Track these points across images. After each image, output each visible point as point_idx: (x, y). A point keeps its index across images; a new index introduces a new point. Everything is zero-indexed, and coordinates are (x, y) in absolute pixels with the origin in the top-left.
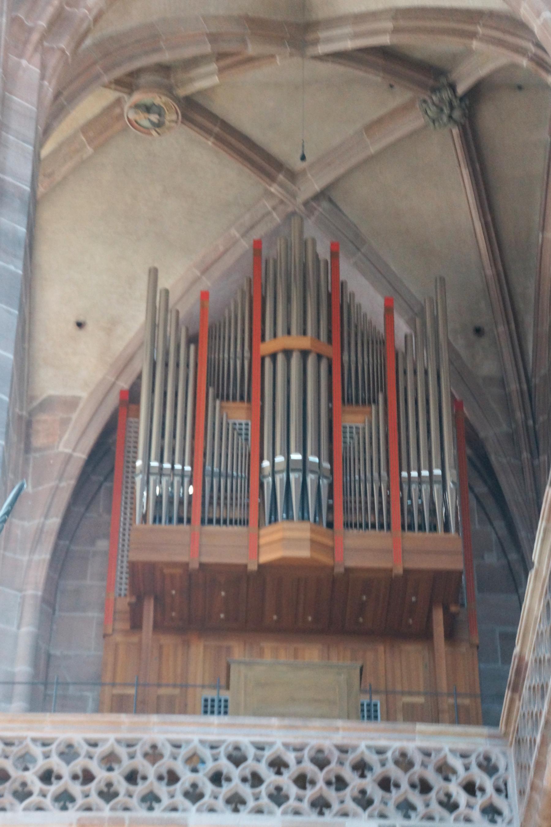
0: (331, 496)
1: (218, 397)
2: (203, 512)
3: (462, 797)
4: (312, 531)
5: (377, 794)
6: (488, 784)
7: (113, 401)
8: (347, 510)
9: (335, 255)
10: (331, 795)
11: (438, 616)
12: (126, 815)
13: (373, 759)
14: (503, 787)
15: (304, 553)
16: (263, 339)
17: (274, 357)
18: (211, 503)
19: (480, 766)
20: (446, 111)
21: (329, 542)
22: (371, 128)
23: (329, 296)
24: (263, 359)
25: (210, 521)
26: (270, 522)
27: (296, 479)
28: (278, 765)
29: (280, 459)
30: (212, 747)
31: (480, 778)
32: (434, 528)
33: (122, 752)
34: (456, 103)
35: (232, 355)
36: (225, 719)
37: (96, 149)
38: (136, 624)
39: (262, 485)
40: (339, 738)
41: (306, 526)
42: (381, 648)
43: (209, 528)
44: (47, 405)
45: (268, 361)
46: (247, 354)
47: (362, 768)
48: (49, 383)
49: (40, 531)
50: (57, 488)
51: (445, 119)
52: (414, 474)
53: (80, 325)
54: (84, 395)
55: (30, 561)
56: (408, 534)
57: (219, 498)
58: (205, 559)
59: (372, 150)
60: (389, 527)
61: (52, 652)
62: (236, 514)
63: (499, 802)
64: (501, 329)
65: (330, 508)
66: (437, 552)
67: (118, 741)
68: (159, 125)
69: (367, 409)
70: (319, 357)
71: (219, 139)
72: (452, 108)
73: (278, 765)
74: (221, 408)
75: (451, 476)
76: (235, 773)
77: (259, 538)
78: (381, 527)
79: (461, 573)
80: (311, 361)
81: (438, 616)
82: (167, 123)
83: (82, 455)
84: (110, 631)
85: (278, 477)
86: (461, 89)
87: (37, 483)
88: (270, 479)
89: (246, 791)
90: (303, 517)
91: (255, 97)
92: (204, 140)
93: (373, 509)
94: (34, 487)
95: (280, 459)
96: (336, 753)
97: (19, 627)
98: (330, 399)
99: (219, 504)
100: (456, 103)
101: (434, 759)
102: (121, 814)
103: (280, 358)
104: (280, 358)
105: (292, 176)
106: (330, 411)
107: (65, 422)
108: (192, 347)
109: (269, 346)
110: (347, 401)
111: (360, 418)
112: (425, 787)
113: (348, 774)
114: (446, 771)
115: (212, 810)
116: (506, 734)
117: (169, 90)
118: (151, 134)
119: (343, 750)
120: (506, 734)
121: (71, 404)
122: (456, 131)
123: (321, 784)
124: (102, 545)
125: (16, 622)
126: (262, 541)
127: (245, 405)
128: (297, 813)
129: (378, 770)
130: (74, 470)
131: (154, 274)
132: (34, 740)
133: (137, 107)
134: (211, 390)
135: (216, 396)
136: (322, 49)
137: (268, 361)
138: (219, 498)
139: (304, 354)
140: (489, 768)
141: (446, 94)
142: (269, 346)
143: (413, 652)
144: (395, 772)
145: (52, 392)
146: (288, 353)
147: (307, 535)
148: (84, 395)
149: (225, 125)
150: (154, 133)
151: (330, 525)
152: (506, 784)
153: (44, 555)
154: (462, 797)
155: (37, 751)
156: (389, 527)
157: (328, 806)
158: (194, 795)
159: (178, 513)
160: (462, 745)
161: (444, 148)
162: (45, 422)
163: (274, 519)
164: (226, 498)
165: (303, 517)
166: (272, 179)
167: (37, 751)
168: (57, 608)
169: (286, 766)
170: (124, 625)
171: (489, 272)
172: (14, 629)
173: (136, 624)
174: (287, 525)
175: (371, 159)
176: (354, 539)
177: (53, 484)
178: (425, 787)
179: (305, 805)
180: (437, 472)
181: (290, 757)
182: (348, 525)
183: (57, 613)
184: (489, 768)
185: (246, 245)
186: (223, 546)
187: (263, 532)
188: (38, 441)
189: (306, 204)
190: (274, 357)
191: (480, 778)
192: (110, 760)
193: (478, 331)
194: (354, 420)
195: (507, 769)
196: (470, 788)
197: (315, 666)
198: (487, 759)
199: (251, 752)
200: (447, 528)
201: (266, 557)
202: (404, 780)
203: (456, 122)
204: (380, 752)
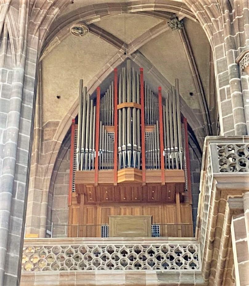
0: (141, 157)
1: (103, 124)
2: (99, 164)
3: (183, 261)
4: (135, 171)
5: (156, 261)
6: (192, 256)
7: (70, 123)
8: (146, 162)
10: (141, 262)
12: (75, 271)
13: (155, 250)
14: (197, 257)
15: (133, 179)
16: (118, 104)
17: (122, 109)
18: (101, 162)
19: (189, 250)
20: (176, 25)
22: (152, 30)
24: (118, 110)
25: (101, 168)
26: (121, 168)
27: (129, 153)
28: (124, 253)
29: (124, 146)
30: (102, 248)
32: (175, 167)
33: (73, 250)
34: (179, 23)
35: (108, 109)
36: (107, 239)
37: (61, 41)
38: (79, 202)
39: (118, 155)
41: (133, 169)
42: (160, 207)
43: (101, 171)
44: (48, 125)
45: (120, 111)
46: (113, 109)
47: (151, 252)
48: (48, 118)
50: (52, 153)
51: (176, 28)
53: (58, 97)
55: (44, 179)
56: (167, 170)
57: (104, 160)
59: (153, 37)
60: (160, 168)
61: (53, 209)
63: (195, 262)
65: (141, 162)
66: (178, 176)
67: (72, 247)
69: (153, 126)
70: (137, 109)
71: (102, 36)
72: (177, 24)
73: (124, 253)
74: (104, 128)
75: (181, 149)
77: (117, 174)
78: (158, 168)
79: (184, 184)
80: (134, 110)
81: (178, 197)
82: (84, 33)
83: (60, 142)
84: (70, 205)
86: (180, 19)
87: (46, 152)
88: (121, 153)
89: (114, 262)
90: (132, 166)
92: (97, 37)
93: (155, 161)
94: (45, 153)
95: (124, 146)
96: (143, 248)
97: (41, 202)
98: (140, 123)
99: (104, 162)
100: (179, 23)
101: (175, 248)
102: (73, 271)
103: (124, 110)
104: (124, 110)
105: (127, 46)
106: (140, 127)
107: (54, 130)
108: (95, 107)
109: (120, 106)
111: (150, 129)
113: (147, 255)
114: (178, 253)
115: (103, 269)
116: (197, 239)
118: (79, 36)
119: (145, 247)
120: (197, 239)
121: (57, 124)
122: (180, 31)
123: (138, 259)
124: (68, 171)
125: (40, 201)
126: (119, 175)
127: (113, 126)
128: (130, 269)
129: (156, 253)
130: (58, 147)
132: (45, 247)
133: (74, 28)
134: (101, 122)
135: (103, 124)
136: (132, 11)
137: (120, 111)
138: (104, 160)
139: (132, 108)
140: (192, 252)
141: (175, 20)
142: (120, 106)
143: (170, 207)
144: (162, 254)
145: (50, 120)
146: (126, 108)
147: (133, 173)
148: (61, 121)
149: (104, 31)
151: (141, 168)
152: (197, 256)
154: (183, 261)
155: (46, 251)
156: (160, 168)
157: (140, 266)
158: (97, 264)
159: (91, 165)
160: (184, 243)
161: (176, 36)
164: (106, 160)
165: (132, 166)
166: (120, 47)
167: (46, 251)
168: (54, 194)
169: (127, 253)
172: (40, 203)
173: (79, 202)
174: (126, 169)
176: (149, 173)
177: (52, 152)
179: (133, 266)
180: (176, 148)
181: (128, 250)
182: (147, 167)
183: (54, 196)
184: (192, 252)
186: (106, 177)
187: (118, 172)
188: (45, 138)
189: (131, 55)
190: (122, 109)
191: (190, 255)
192: (69, 254)
193: (191, 94)
194: (149, 130)
195: (198, 251)
196: (186, 258)
198: (192, 247)
199: (115, 249)
200: (180, 168)
201: (119, 182)
202: (164, 256)
203: (179, 28)
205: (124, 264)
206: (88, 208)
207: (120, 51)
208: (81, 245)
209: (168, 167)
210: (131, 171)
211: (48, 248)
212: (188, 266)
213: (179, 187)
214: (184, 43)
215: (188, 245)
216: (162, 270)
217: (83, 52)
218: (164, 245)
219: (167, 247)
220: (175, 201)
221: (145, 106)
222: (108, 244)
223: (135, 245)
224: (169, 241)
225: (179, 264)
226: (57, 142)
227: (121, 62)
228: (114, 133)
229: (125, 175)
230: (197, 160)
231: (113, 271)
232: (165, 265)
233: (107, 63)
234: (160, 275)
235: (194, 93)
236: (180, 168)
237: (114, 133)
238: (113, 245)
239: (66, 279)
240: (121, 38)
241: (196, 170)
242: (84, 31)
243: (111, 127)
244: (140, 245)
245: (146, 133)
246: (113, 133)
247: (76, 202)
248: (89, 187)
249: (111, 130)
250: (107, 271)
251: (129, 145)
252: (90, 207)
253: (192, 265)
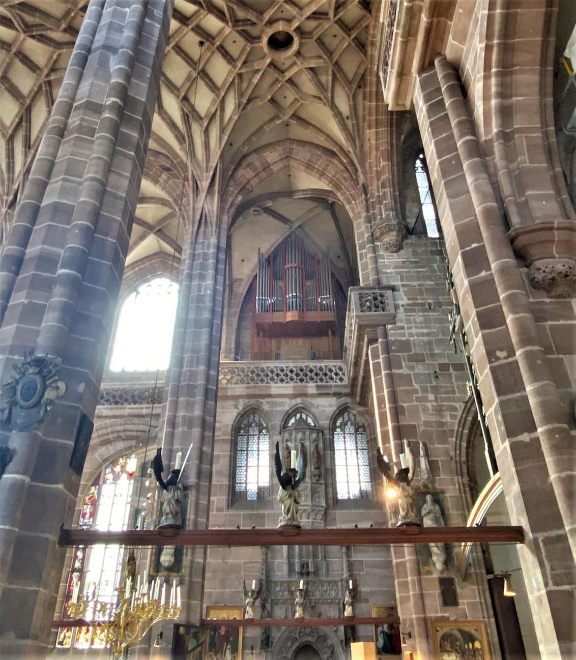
3: (334, 377)
5: (315, 377)
7: (251, 279)
10: (304, 378)
13: (314, 369)
22: (310, 211)
28: (292, 371)
31: (339, 372)
40: (306, 364)
47: (311, 371)
48: (236, 275)
49: (236, 312)
54: (244, 277)
58: (275, 321)
63: (343, 377)
66: (330, 316)
73: (292, 371)
76: (282, 374)
83: (245, 293)
89: (284, 378)
90: (296, 309)
91: (282, 206)
107: (240, 285)
109: (287, 266)
112: (326, 375)
114: (331, 371)
117: (260, 206)
121: (242, 280)
124: (251, 314)
133: (254, 211)
139: (296, 268)
143: (325, 338)
144: (319, 372)
146: (292, 268)
153: (237, 318)
154: (334, 377)
155: (236, 370)
158: (272, 379)
160: (335, 364)
161: (327, 215)
162: (235, 285)
163: (289, 310)
167: (236, 370)
170: (255, 336)
173: (259, 335)
178: (326, 375)
181: (294, 370)
182: (307, 310)
184: (341, 369)
186: (277, 317)
188: (234, 289)
191: (339, 372)
194: (309, 283)
196: (336, 374)
197: (300, 344)
199: (285, 369)
201: (288, 320)
202: (321, 373)
204: (316, 367)
205: (292, 379)
211: (237, 368)
212: (338, 380)
213: (330, 324)
216: (320, 383)
220: (327, 335)
222: (280, 365)
225: (331, 379)
226: (269, 166)
229: (291, 316)
231: (284, 384)
232: (321, 380)
234: (318, 387)
239: (250, 390)
249: (281, 284)
250: (280, 384)
252: (267, 340)
253: (341, 380)
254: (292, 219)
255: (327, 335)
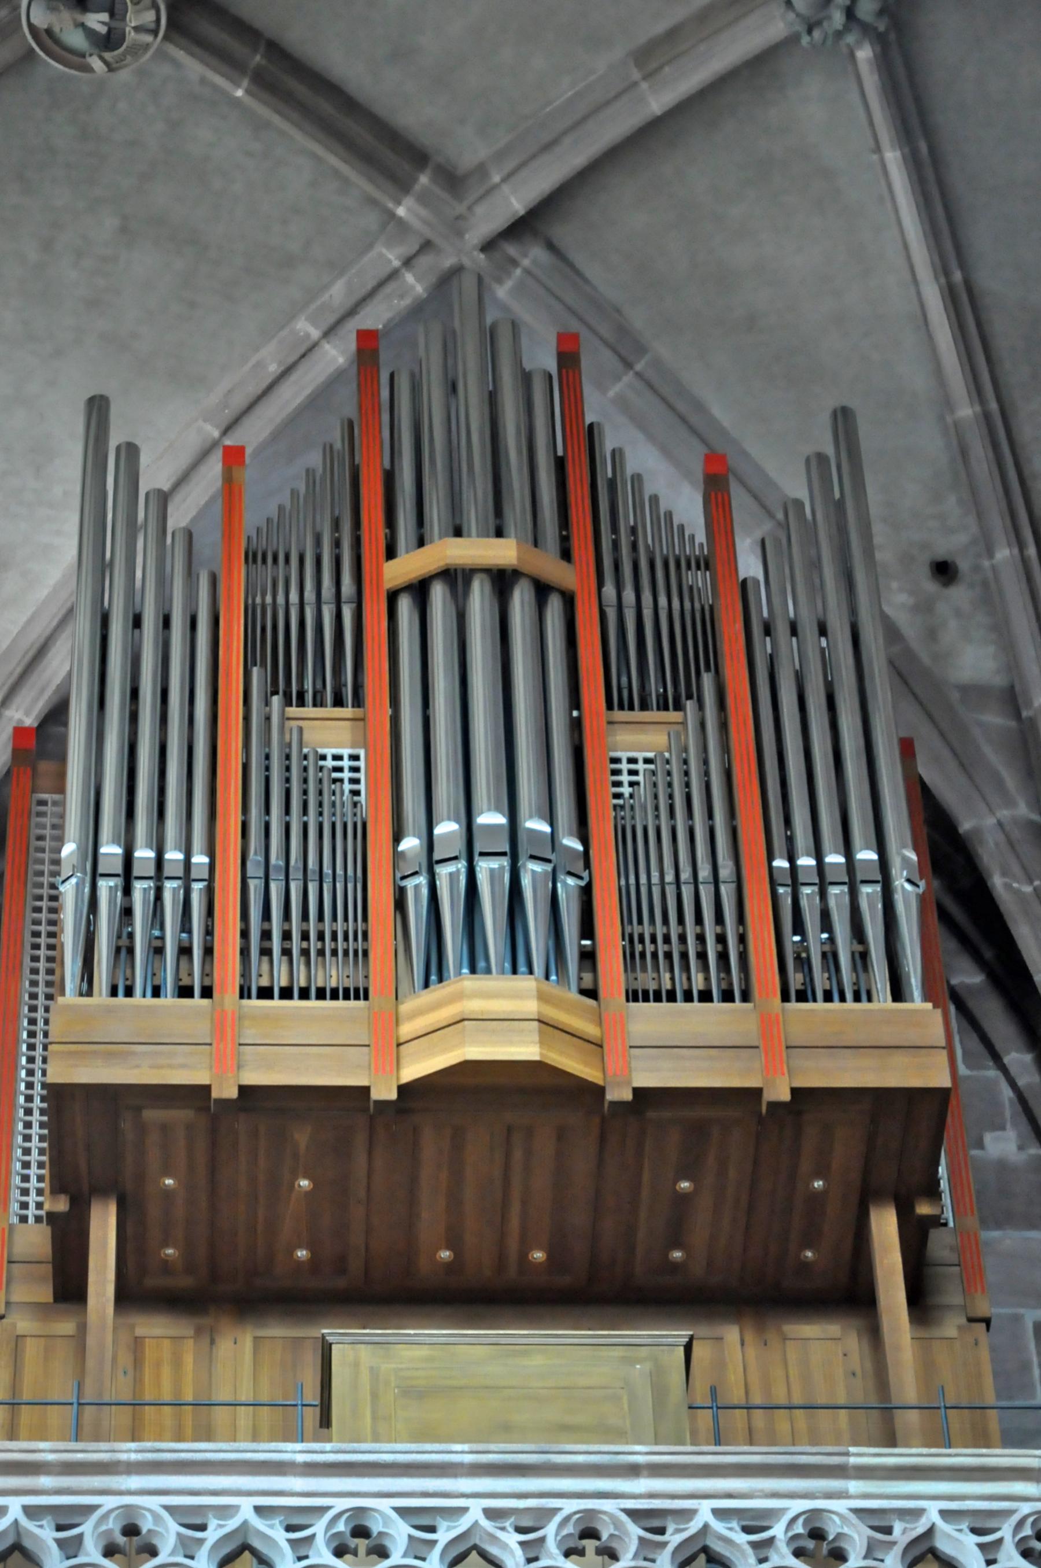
0: (587, 929)
1: (275, 692)
8: (632, 959)
9: (568, 358)
11: (885, 1227)
21: (591, 1030)
23: (560, 465)
24: (393, 597)
29: (447, 828)
41: (526, 983)
42: (731, 1333)
45: (405, 606)
52: (806, 861)
58: (253, 1078)
59: (657, 104)
62: (332, 975)
64: (1004, 553)
67: (30, 1512)
68: (109, 41)
69: (673, 716)
70: (542, 590)
71: (263, 83)
77: (397, 1024)
80: (521, 598)
81: (885, 1227)
82: (131, 36)
85: (443, 871)
88: (422, 880)
95: (447, 828)
96: (635, 1531)
98: (575, 699)
101: (902, 1533)
103: (438, 593)
105: (453, 181)
106: (576, 726)
110: (616, 700)
118: (88, 69)
131: (98, 409)
139: (503, 581)
142: (408, 566)
146: (456, 578)
147: (531, 1007)
150: (96, 64)
163: (435, 970)
165: (517, 960)
171: (966, 411)
174: (470, 983)
175: (654, 126)
180: (867, 855)
185: (337, 355)
187: (405, 1008)
189: (488, 246)
190: (420, 590)
193: (944, 571)
194: (639, 742)
203: (866, 29)
206: (139, 1331)
207: (401, 211)
208: (109, 1502)
209: (802, 997)
210: (517, 995)
214: (893, 157)
215: (1010, 1513)
217: (110, 223)
218: (814, 1514)
219: (833, 1528)
220: (850, 1295)
221: (600, 584)
223: (570, 1506)
224: (854, 1486)
227: (407, 301)
228: (362, 753)
230: (992, 1073)
233: (292, 317)
235: (964, 565)
236: (898, 993)
237: (362, 753)
238: (385, 1505)
240: (417, 114)
241: (988, 1138)
242: (133, 20)
243: (338, 712)
244: (607, 1505)
245: (616, 760)
246: (355, 758)
247: (45, 1293)
248: (165, 1128)
251: (490, 818)
254: (468, 150)
255: (850, 1295)
